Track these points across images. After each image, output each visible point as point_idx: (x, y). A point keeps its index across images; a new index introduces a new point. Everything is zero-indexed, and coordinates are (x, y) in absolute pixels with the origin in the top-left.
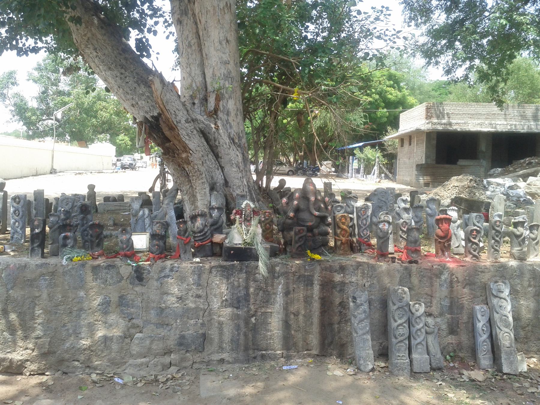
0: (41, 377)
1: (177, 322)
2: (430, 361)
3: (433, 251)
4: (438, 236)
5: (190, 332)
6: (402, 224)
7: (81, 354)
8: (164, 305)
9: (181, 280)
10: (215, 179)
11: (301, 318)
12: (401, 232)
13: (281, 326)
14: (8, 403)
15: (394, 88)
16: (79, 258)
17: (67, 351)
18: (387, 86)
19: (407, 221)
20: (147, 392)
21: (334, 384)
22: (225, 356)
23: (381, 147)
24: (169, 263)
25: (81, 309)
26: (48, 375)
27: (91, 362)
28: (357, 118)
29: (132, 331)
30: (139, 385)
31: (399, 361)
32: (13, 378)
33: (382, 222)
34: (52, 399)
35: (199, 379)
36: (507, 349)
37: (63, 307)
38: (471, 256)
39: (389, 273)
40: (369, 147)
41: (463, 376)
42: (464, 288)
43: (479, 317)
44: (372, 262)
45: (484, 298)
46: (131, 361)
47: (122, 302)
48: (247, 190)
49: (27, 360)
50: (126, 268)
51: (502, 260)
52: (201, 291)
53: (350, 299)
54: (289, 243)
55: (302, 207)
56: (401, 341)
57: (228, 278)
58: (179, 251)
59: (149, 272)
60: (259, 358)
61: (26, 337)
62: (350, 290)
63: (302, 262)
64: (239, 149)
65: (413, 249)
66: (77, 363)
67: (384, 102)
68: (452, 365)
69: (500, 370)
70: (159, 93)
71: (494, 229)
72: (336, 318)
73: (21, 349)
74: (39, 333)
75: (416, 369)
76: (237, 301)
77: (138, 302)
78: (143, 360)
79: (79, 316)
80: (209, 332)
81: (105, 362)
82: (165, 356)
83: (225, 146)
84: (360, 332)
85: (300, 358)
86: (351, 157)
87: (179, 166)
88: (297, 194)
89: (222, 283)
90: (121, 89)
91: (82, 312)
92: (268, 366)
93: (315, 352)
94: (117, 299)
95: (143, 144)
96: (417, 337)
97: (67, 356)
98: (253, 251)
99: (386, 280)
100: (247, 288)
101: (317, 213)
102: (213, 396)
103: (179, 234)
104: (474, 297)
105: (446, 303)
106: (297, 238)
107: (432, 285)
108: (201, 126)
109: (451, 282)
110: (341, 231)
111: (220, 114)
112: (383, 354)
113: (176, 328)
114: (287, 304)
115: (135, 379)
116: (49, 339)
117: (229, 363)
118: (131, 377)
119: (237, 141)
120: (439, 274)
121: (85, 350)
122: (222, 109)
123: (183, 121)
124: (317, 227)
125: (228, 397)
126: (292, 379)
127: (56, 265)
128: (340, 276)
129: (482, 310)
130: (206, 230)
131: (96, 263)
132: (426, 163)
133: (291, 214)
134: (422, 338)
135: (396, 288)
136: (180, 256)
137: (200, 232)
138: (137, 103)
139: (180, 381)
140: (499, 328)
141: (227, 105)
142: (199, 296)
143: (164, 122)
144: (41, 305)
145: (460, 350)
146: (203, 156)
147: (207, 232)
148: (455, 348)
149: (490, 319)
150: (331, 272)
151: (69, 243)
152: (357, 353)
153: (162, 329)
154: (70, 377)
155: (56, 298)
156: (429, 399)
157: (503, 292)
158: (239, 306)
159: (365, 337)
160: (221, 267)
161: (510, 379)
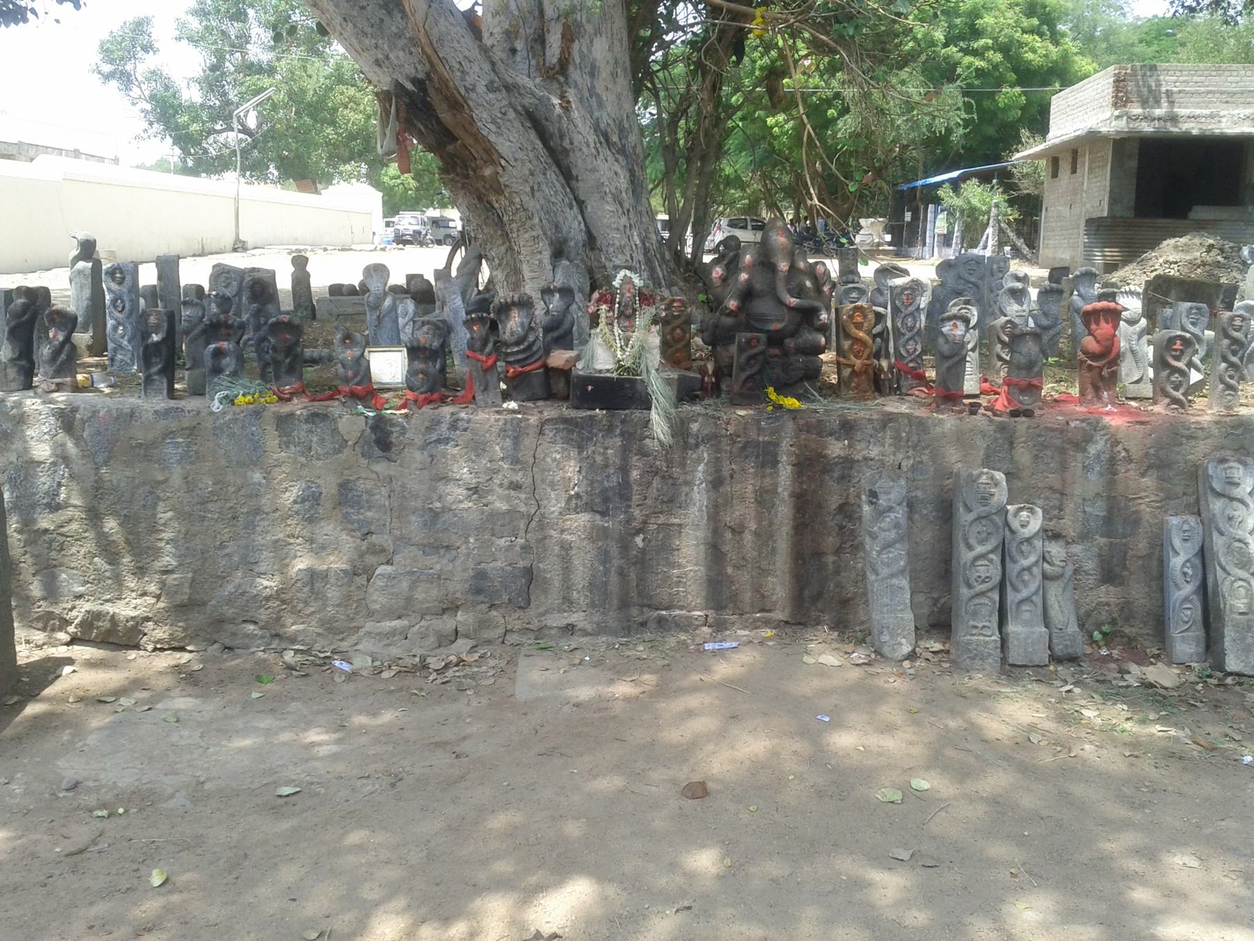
0: (178, 655)
1: (467, 542)
2: (1050, 640)
3: (1075, 391)
4: (1085, 353)
5: (499, 564)
7: (260, 607)
8: (438, 505)
9: (475, 449)
10: (565, 230)
11: (748, 537)
12: (999, 346)
13: (702, 554)
14: (106, 702)
15: (1041, 35)
16: (249, 398)
17: (229, 601)
18: (1024, 32)
19: (1017, 321)
20: (401, 689)
21: (816, 683)
22: (576, 618)
23: (1006, 180)
24: (446, 411)
25: (257, 511)
26: (191, 652)
27: (283, 626)
29: (370, 560)
30: (385, 675)
31: (974, 638)
32: (120, 654)
33: (950, 319)
34: (196, 697)
35: (516, 665)
36: (1238, 617)
37: (219, 504)
38: (1167, 401)
39: (960, 439)
40: (975, 181)
41: (1126, 677)
42: (1143, 475)
43: (1177, 542)
44: (922, 413)
45: (1192, 499)
46: (369, 626)
47: (346, 496)
48: (641, 258)
49: (148, 619)
50: (351, 420)
51: (1243, 411)
52: (520, 474)
53: (864, 497)
54: (726, 371)
55: (758, 286)
56: (982, 594)
57: (581, 448)
58: (471, 387)
59: (404, 430)
60: (652, 625)
61: (141, 568)
62: (864, 477)
63: (751, 412)
64: (620, 158)
65: (1025, 383)
66: (252, 627)
67: (1015, 70)
68: (1104, 652)
69: (1219, 665)
70: (420, 16)
71: (1227, 336)
72: (831, 541)
73: (134, 594)
74: (168, 560)
75: (1015, 656)
76: (604, 499)
77: (381, 496)
78: (396, 623)
79: (250, 526)
80: (541, 565)
81: (313, 627)
82: (445, 617)
83: (585, 150)
84: (885, 572)
85: (744, 628)
86: (931, 207)
87: (480, 199)
88: (748, 257)
89: (569, 458)
90: (350, 25)
91: (258, 518)
92: (672, 641)
93: (779, 615)
94: (334, 491)
95: (394, 146)
96: (1020, 586)
97: (230, 612)
98: (639, 387)
99: (952, 456)
100: (624, 470)
101: (793, 301)
102: (538, 699)
103: (471, 346)
104: (1167, 498)
105: (1098, 510)
106: (744, 357)
107: (1064, 467)
108: (528, 101)
109: (1112, 461)
110: (852, 345)
111: (574, 74)
112: (940, 623)
113: (468, 555)
114: (716, 506)
115: (377, 663)
116: (190, 575)
117: (585, 633)
118: (369, 659)
119: (615, 138)
120: (1081, 443)
121: (268, 599)
122: (578, 61)
123: (481, 88)
124: (793, 334)
125: (575, 700)
126: (722, 670)
127: (198, 413)
128: (840, 445)
129: (1186, 527)
130: (531, 338)
131: (285, 409)
132: (1112, 216)
133: (732, 304)
134: (1033, 587)
135: (975, 472)
136: (474, 397)
137: (517, 343)
138: (387, 57)
139: (476, 669)
140: (1224, 569)
141: (590, 51)
142: (516, 487)
143: (438, 91)
144: (171, 501)
145: (1127, 619)
146: (532, 174)
147: (533, 344)
148: (1116, 615)
149: (1202, 549)
150: (819, 434)
151: (228, 366)
152: (876, 616)
153: (435, 558)
154: (238, 656)
155: (200, 485)
156: (1035, 720)
157: (1238, 485)
158: (608, 508)
159: (895, 581)
160: (565, 421)
161: (1240, 684)
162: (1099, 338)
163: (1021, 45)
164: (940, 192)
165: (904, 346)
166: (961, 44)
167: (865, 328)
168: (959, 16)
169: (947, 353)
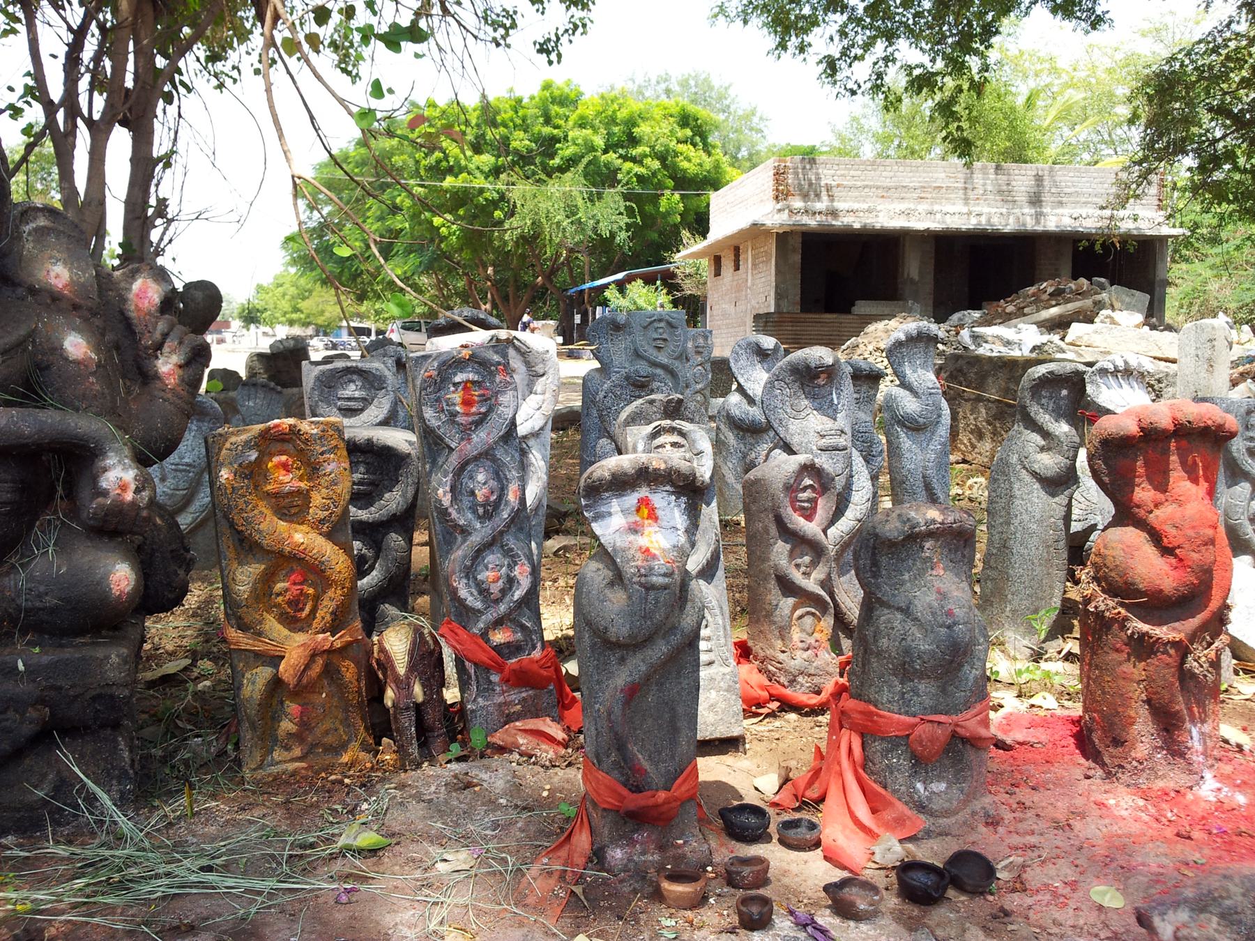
6: (791, 489)
15: (694, 145)
18: (679, 142)
19: (824, 462)
23: (669, 281)
28: (610, 216)
33: (621, 484)
40: (640, 282)
110: (267, 579)
162: (1172, 535)
163: (676, 154)
164: (607, 294)
165: (469, 572)
166: (621, 151)
167: (315, 512)
168: (617, 124)
169: (620, 630)
